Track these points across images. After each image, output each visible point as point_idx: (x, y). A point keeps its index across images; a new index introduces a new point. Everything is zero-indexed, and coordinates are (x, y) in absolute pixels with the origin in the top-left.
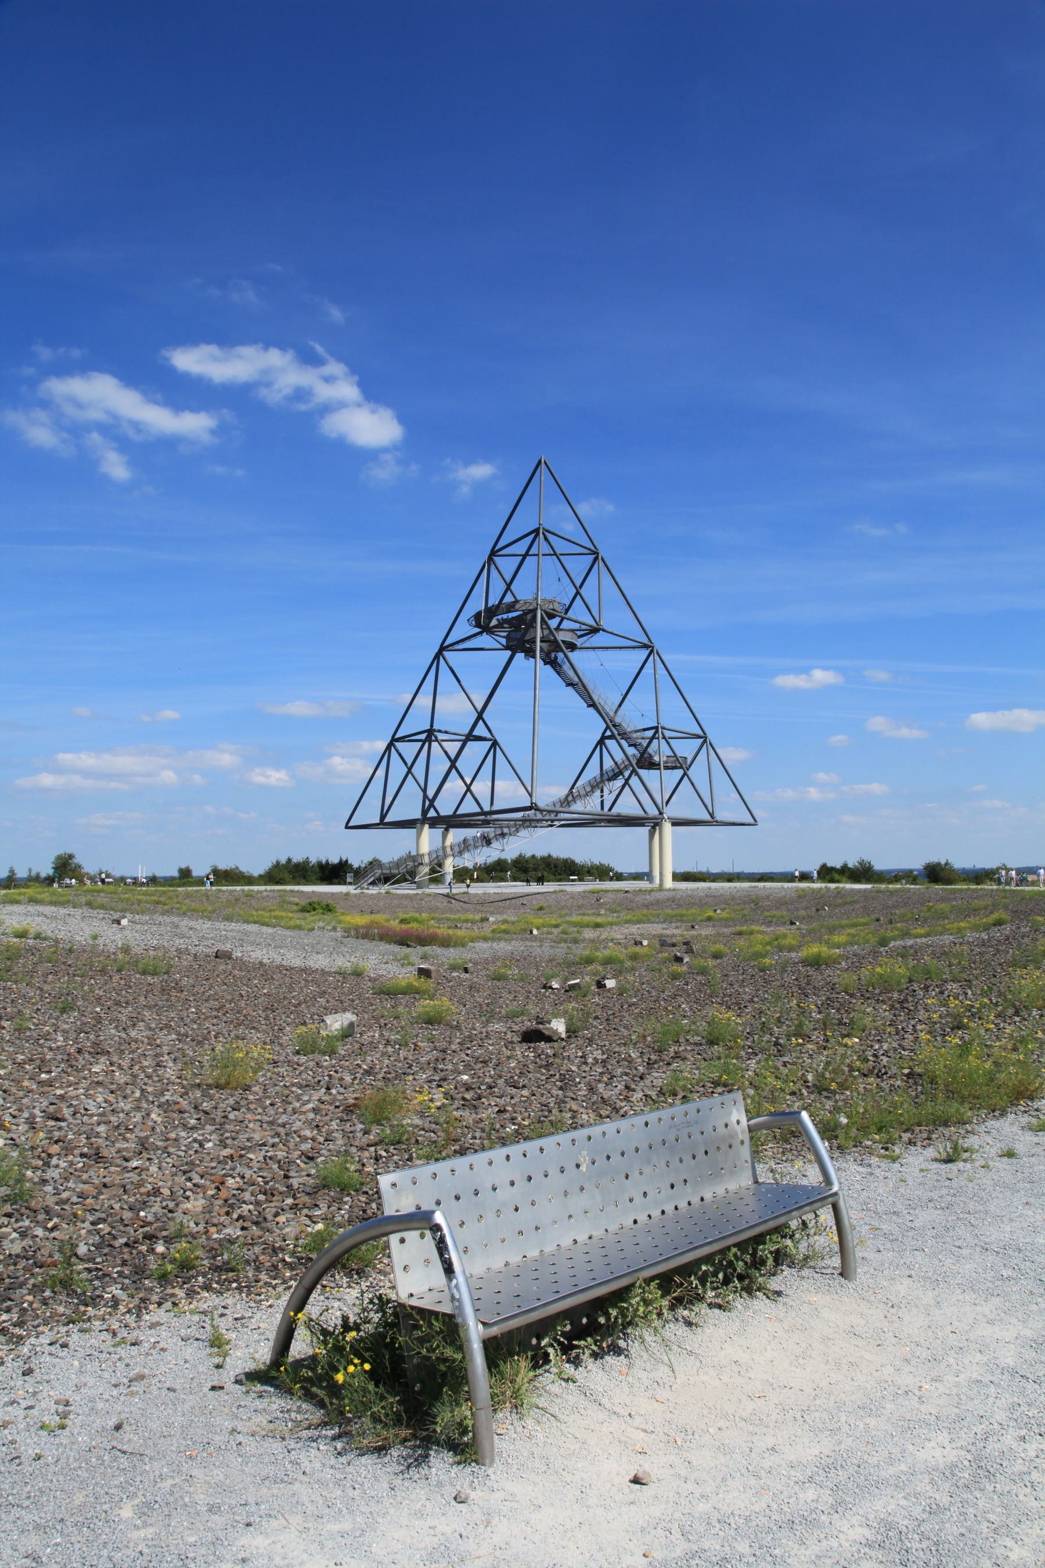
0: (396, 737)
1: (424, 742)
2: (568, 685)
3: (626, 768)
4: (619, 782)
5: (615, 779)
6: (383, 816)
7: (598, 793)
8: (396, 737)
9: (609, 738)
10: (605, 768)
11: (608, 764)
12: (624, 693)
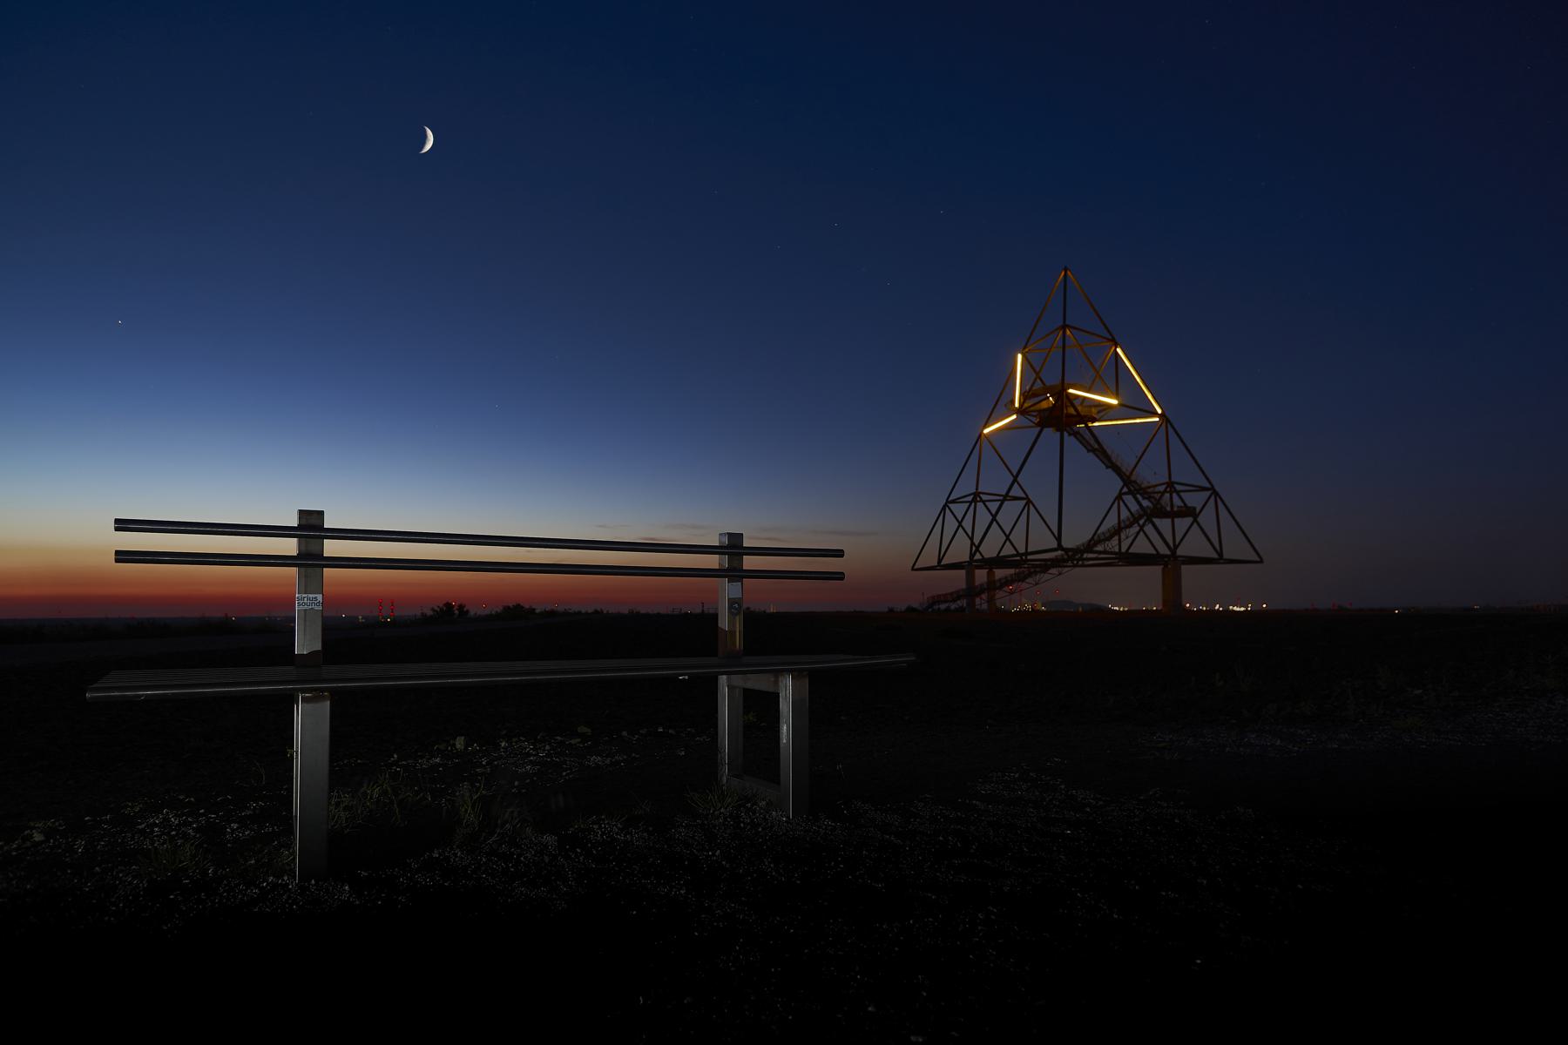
0: (950, 499)
3: (1141, 517)
4: (1135, 529)
6: (940, 560)
7: (1117, 537)
8: (950, 499)
9: (1125, 494)
10: (1122, 518)
11: (1125, 514)
12: (1139, 456)
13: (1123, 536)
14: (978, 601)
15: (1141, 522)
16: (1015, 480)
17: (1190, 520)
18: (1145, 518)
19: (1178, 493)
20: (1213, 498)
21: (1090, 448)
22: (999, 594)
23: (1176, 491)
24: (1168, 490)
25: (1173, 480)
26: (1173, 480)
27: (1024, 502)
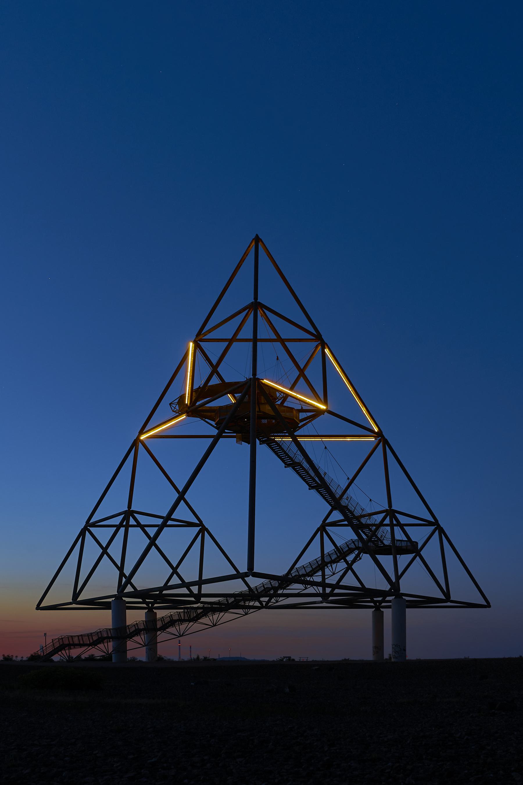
1: (118, 527)
2: (287, 465)
3: (351, 551)
4: (342, 565)
5: (338, 562)
6: (76, 595)
7: (320, 573)
9: (334, 524)
10: (326, 552)
11: (329, 548)
12: (351, 478)
13: (328, 571)
14: (130, 644)
15: (350, 558)
16: (181, 496)
17: (409, 557)
18: (356, 552)
19: (402, 526)
20: (437, 533)
21: (289, 462)
22: (161, 636)
23: (399, 524)
24: (387, 521)
25: (394, 508)
26: (394, 508)
27: (198, 529)
